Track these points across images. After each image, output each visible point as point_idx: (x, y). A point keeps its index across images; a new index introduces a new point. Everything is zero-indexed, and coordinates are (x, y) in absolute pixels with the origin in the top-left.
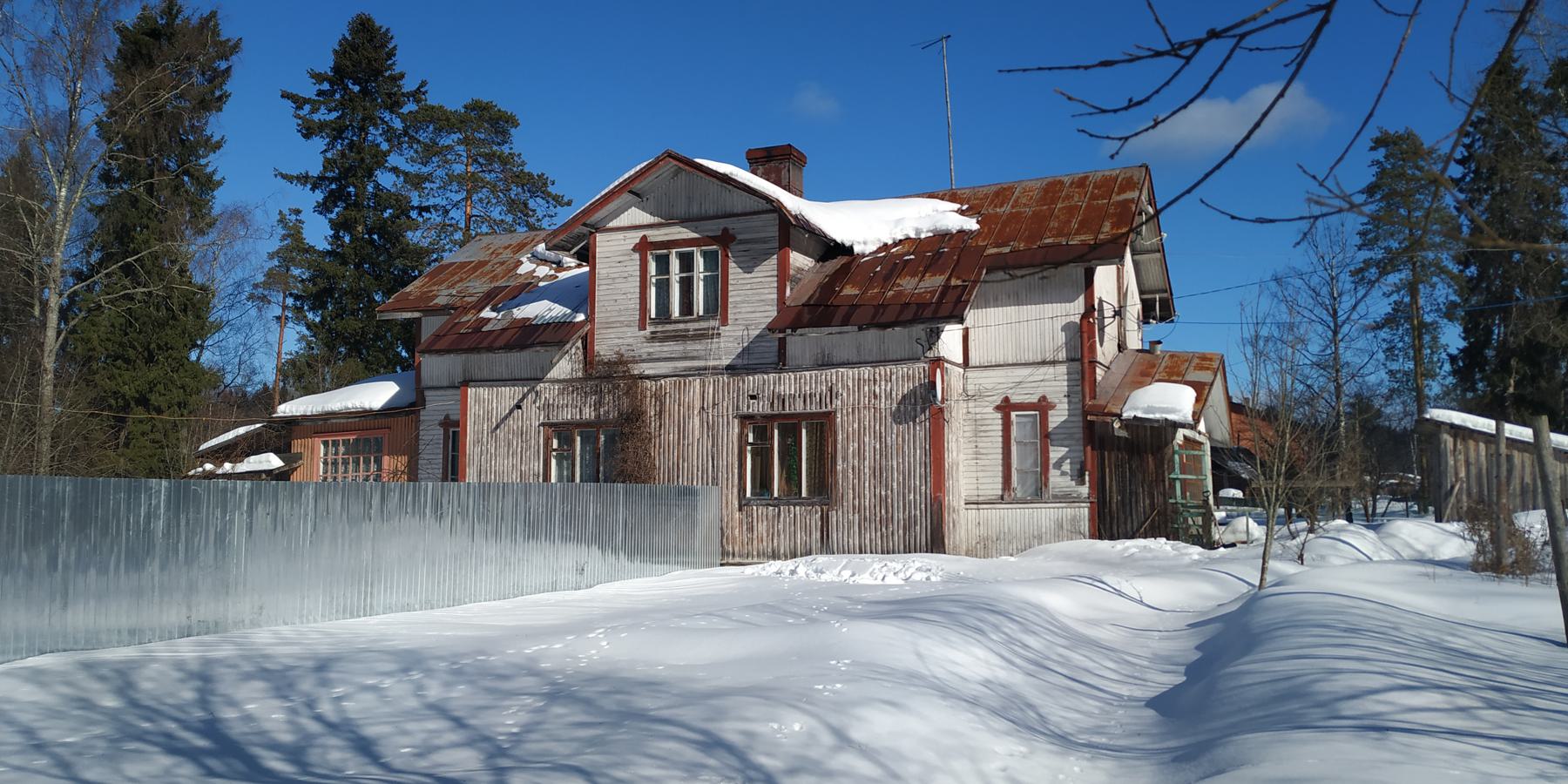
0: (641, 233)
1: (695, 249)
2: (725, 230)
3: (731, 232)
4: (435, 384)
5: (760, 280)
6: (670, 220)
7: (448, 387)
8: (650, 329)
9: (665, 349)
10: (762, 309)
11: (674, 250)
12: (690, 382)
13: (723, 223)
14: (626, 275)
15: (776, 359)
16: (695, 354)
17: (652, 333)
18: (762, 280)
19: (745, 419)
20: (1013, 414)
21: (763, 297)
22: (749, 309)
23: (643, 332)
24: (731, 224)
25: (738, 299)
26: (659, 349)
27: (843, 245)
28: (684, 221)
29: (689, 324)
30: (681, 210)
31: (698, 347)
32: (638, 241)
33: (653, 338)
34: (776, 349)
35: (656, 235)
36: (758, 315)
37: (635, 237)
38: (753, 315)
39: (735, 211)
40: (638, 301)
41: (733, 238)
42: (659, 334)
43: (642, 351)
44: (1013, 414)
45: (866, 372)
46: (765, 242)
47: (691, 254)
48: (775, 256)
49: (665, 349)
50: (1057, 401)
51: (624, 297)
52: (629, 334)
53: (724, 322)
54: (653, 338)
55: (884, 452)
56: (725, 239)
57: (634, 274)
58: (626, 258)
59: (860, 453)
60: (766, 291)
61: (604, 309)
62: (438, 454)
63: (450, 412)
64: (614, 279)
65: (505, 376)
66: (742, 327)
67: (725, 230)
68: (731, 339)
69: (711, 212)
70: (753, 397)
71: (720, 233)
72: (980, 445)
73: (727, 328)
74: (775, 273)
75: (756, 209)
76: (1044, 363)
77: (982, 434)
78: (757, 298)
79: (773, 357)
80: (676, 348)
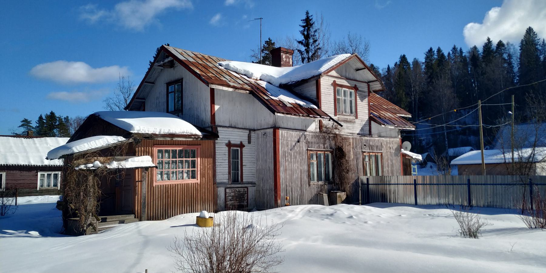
0: (334, 79)
2: (356, 85)
4: (222, 124)
6: (342, 77)
7: (229, 127)
10: (365, 115)
11: (343, 89)
13: (354, 83)
14: (329, 94)
24: (358, 84)
28: (347, 79)
30: (344, 74)
35: (339, 81)
45: (388, 139)
46: (365, 93)
48: (367, 98)
51: (329, 102)
53: (357, 117)
55: (392, 165)
56: (356, 88)
62: (226, 160)
63: (231, 140)
64: (326, 94)
65: (292, 128)
66: (361, 121)
70: (365, 145)
79: (368, 133)
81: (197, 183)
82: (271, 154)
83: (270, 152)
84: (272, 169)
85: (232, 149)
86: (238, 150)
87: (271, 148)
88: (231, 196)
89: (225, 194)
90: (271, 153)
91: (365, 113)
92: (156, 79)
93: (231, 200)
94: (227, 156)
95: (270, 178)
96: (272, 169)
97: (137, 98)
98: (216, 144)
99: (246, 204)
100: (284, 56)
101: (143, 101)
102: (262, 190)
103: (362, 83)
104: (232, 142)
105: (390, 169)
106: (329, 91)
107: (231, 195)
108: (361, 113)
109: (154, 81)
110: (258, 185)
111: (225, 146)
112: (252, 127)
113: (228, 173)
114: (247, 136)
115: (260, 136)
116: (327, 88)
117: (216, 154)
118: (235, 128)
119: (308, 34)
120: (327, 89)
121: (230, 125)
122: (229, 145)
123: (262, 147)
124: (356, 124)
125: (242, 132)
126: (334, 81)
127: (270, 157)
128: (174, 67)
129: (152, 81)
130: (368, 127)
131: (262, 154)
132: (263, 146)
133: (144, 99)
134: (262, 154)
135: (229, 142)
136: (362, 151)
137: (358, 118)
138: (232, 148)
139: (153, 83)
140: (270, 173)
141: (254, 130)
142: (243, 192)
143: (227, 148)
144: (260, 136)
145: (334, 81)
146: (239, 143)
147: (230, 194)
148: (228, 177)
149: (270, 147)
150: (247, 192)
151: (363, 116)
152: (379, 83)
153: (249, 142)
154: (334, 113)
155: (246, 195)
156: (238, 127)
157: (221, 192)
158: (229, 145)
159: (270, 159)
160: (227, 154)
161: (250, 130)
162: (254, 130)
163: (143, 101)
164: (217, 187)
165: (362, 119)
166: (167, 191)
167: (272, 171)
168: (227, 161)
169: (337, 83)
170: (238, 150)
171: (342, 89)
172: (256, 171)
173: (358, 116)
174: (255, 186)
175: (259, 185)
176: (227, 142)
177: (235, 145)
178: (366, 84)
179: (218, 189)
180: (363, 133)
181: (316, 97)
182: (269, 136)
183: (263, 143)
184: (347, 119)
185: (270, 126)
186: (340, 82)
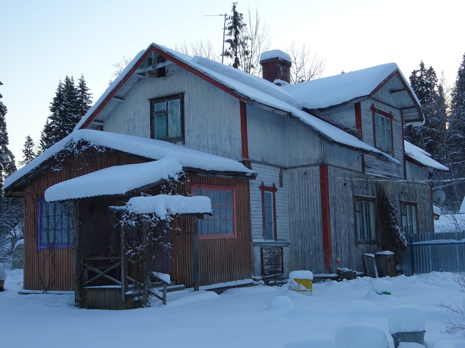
2: (391, 112)
11: (380, 115)
39: (405, 106)
63: (263, 180)
69: (387, 102)
71: (389, 113)
81: (234, 239)
82: (317, 201)
83: (314, 198)
84: (318, 221)
86: (270, 194)
87: (316, 192)
88: (267, 259)
89: (262, 256)
90: (317, 199)
92: (128, 93)
93: (267, 265)
94: (261, 202)
95: (315, 234)
96: (318, 221)
97: (95, 121)
98: (250, 186)
99: (281, 270)
100: (281, 69)
101: (101, 124)
102: (302, 250)
105: (424, 226)
107: (267, 257)
109: (124, 95)
110: (294, 243)
111: (258, 189)
112: (282, 164)
113: (262, 226)
114: (278, 175)
115: (296, 176)
116: (367, 114)
117: (251, 199)
119: (236, 40)
120: (366, 115)
122: (263, 188)
123: (299, 191)
125: (273, 170)
127: (314, 205)
128: (165, 75)
129: (122, 96)
130: (403, 169)
131: (300, 200)
132: (301, 191)
133: (102, 122)
134: (300, 200)
136: (400, 200)
139: (122, 98)
140: (315, 227)
141: (285, 168)
142: (278, 253)
143: (260, 192)
144: (296, 176)
145: (373, 105)
147: (266, 255)
148: (263, 232)
149: (313, 191)
150: (281, 254)
152: (416, 110)
153: (281, 185)
155: (281, 257)
157: (257, 253)
158: (263, 188)
159: (314, 207)
160: (260, 199)
161: (283, 168)
162: (285, 168)
163: (101, 124)
164: (253, 246)
166: (232, 244)
167: (318, 223)
168: (261, 209)
169: (375, 107)
170: (270, 194)
172: (290, 224)
174: (287, 246)
175: (295, 244)
177: (268, 189)
178: (399, 111)
179: (254, 249)
181: (355, 126)
182: (311, 174)
183: (302, 186)
185: (313, 163)
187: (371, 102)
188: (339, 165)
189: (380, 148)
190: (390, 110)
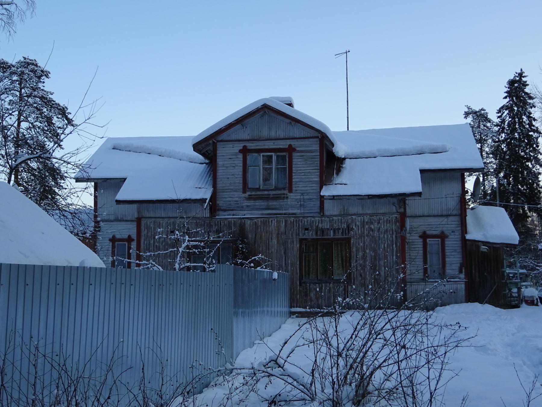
1: (273, 154)
2: (290, 145)
3: (293, 146)
5: (309, 171)
8: (248, 193)
9: (257, 204)
11: (261, 154)
12: (272, 221)
13: (289, 142)
14: (234, 165)
15: (319, 211)
16: (274, 207)
17: (249, 195)
18: (311, 171)
19: (301, 241)
20: (428, 240)
21: (311, 180)
22: (303, 186)
23: (243, 195)
24: (294, 143)
25: (297, 180)
26: (253, 204)
27: (334, 153)
29: (270, 192)
31: (275, 203)
32: (242, 148)
33: (250, 198)
34: (319, 205)
36: (308, 188)
37: (240, 146)
38: (306, 188)
40: (242, 179)
41: (294, 150)
42: (253, 196)
43: (244, 204)
44: (428, 240)
46: (312, 152)
47: (271, 156)
49: (257, 204)
50: (449, 234)
52: (236, 196)
53: (290, 191)
54: (249, 198)
57: (239, 165)
58: (234, 157)
59: (364, 257)
60: (313, 177)
61: (221, 182)
63: (115, 233)
66: (300, 194)
67: (290, 145)
68: (293, 200)
70: (307, 229)
72: (412, 254)
73: (291, 194)
74: (319, 168)
75: (307, 136)
76: (442, 216)
77: (412, 249)
78: (307, 180)
80: (263, 204)
85: (117, 244)
86: (125, 244)
91: (311, 182)
103: (307, 140)
104: (118, 236)
106: (235, 162)
108: (301, 183)
111: (108, 241)
116: (230, 159)
118: (124, 221)
120: (230, 160)
121: (115, 218)
122: (113, 240)
124: (289, 200)
125: (131, 224)
126: (245, 147)
135: (114, 237)
137: (293, 191)
138: (116, 243)
146: (126, 237)
151: (306, 187)
154: (242, 190)
156: (126, 219)
158: (113, 240)
165: (303, 192)
169: (249, 148)
171: (260, 155)
173: (294, 189)
176: (111, 237)
180: (302, 211)
184: (270, 195)
186: (257, 146)
187: (243, 145)
188: (163, 215)
189: (258, 187)
190: (289, 143)
